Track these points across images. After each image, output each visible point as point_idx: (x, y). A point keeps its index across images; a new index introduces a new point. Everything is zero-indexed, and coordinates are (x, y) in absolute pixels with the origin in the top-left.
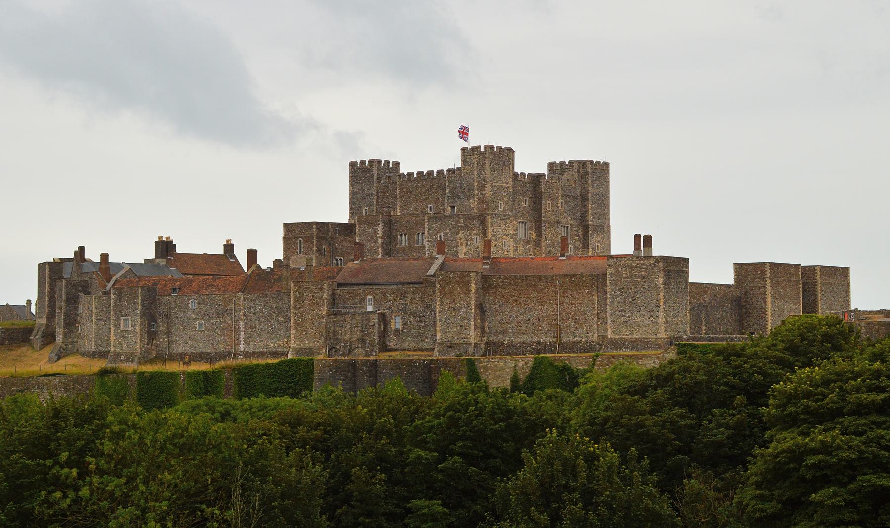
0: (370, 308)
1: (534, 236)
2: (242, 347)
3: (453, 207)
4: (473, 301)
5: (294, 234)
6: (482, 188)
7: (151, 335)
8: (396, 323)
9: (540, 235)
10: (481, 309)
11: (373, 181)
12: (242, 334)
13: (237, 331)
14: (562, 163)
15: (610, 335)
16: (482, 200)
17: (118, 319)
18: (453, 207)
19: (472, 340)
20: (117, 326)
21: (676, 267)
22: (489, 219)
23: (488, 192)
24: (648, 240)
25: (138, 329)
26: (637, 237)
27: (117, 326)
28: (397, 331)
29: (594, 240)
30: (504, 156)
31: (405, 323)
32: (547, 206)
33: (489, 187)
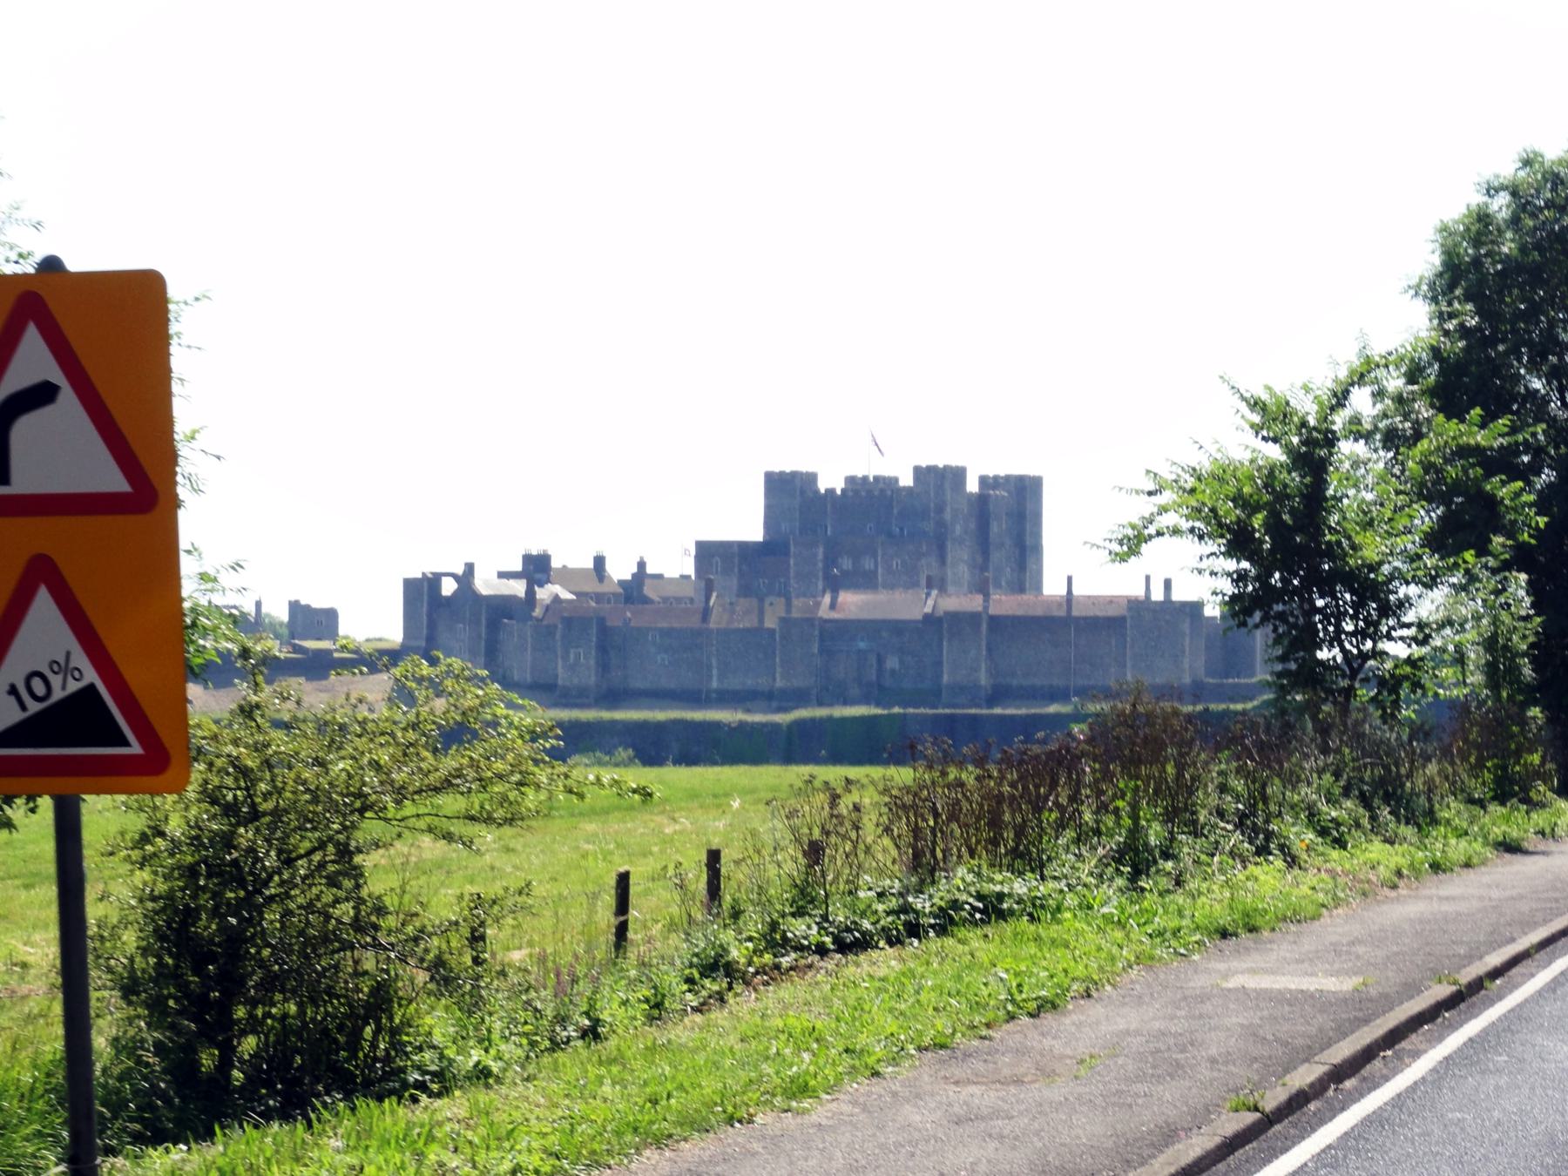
0: (862, 645)
1: (979, 560)
2: (715, 684)
3: (902, 530)
4: (984, 643)
5: (707, 553)
6: (940, 509)
7: (604, 667)
8: (892, 663)
10: (989, 650)
11: (788, 493)
12: (715, 672)
13: (709, 667)
14: (996, 478)
15: (1129, 677)
16: (941, 524)
17: (567, 653)
18: (902, 530)
19: (983, 682)
20: (565, 657)
21: (1196, 607)
22: (949, 544)
23: (948, 516)
24: (1168, 584)
25: (592, 662)
26: (1148, 578)
27: (565, 657)
28: (893, 671)
29: (1031, 565)
30: (958, 474)
31: (901, 662)
32: (994, 528)
33: (948, 509)
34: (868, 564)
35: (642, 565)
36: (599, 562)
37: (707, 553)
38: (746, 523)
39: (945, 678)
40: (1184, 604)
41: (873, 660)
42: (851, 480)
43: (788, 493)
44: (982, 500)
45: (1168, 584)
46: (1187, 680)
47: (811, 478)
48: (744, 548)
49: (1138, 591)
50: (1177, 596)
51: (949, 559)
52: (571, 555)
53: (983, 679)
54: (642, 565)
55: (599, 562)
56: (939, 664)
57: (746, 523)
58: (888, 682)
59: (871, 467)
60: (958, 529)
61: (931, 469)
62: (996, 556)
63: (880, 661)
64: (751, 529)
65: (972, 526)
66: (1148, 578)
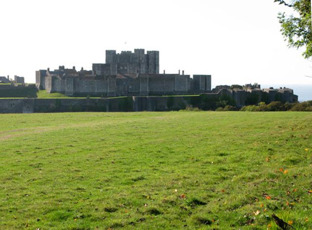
0: (124, 84)
2: (96, 91)
5: (94, 66)
6: (139, 58)
7: (74, 88)
8: (130, 87)
9: (148, 66)
10: (149, 84)
11: (110, 54)
15: (176, 90)
16: (140, 60)
21: (189, 76)
22: (141, 65)
24: (183, 71)
26: (179, 71)
28: (130, 89)
29: (157, 68)
30: (143, 50)
32: (150, 61)
34: (126, 68)
35: (82, 68)
36: (74, 67)
37: (94, 66)
38: (102, 60)
39: (141, 90)
40: (186, 76)
41: (126, 86)
42: (122, 52)
43: (110, 54)
44: (147, 55)
45: (183, 71)
46: (187, 90)
47: (115, 51)
48: (102, 65)
49: (178, 73)
50: (185, 74)
51: (141, 66)
52: (68, 66)
53: (148, 90)
54: (82, 68)
55: (74, 67)
56: (139, 87)
57: (102, 60)
58: (129, 91)
59: (126, 49)
60: (143, 61)
61: (138, 50)
62: (150, 66)
63: (128, 87)
64: (103, 62)
65: (146, 61)
66: (179, 71)
